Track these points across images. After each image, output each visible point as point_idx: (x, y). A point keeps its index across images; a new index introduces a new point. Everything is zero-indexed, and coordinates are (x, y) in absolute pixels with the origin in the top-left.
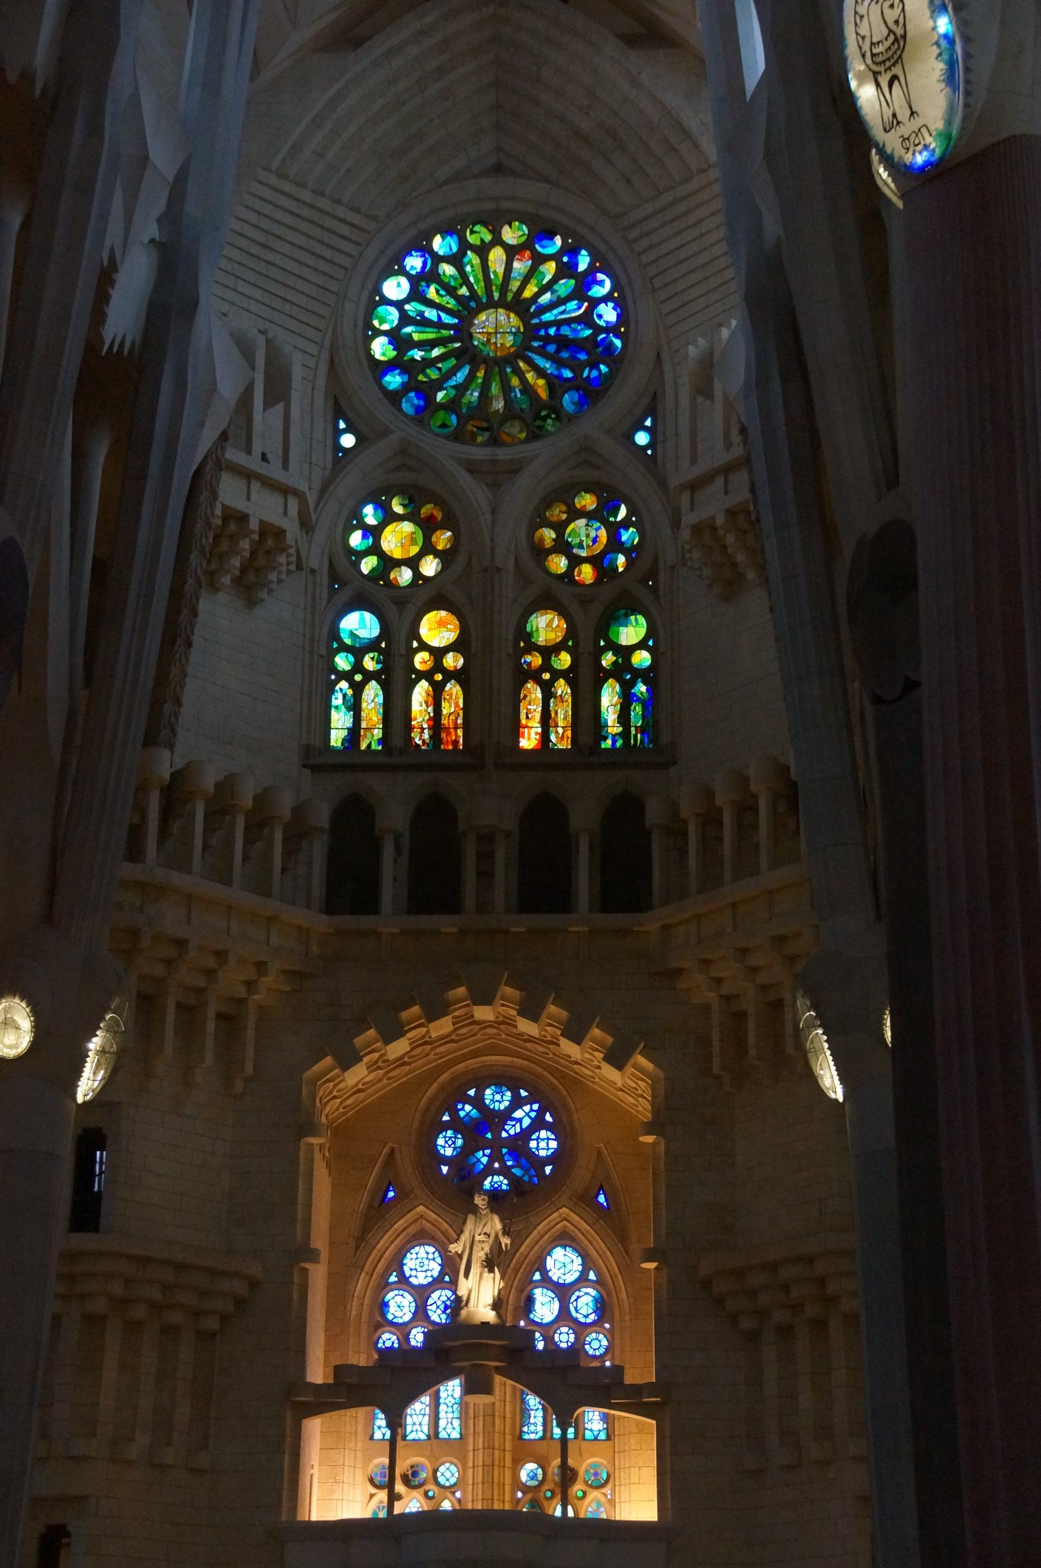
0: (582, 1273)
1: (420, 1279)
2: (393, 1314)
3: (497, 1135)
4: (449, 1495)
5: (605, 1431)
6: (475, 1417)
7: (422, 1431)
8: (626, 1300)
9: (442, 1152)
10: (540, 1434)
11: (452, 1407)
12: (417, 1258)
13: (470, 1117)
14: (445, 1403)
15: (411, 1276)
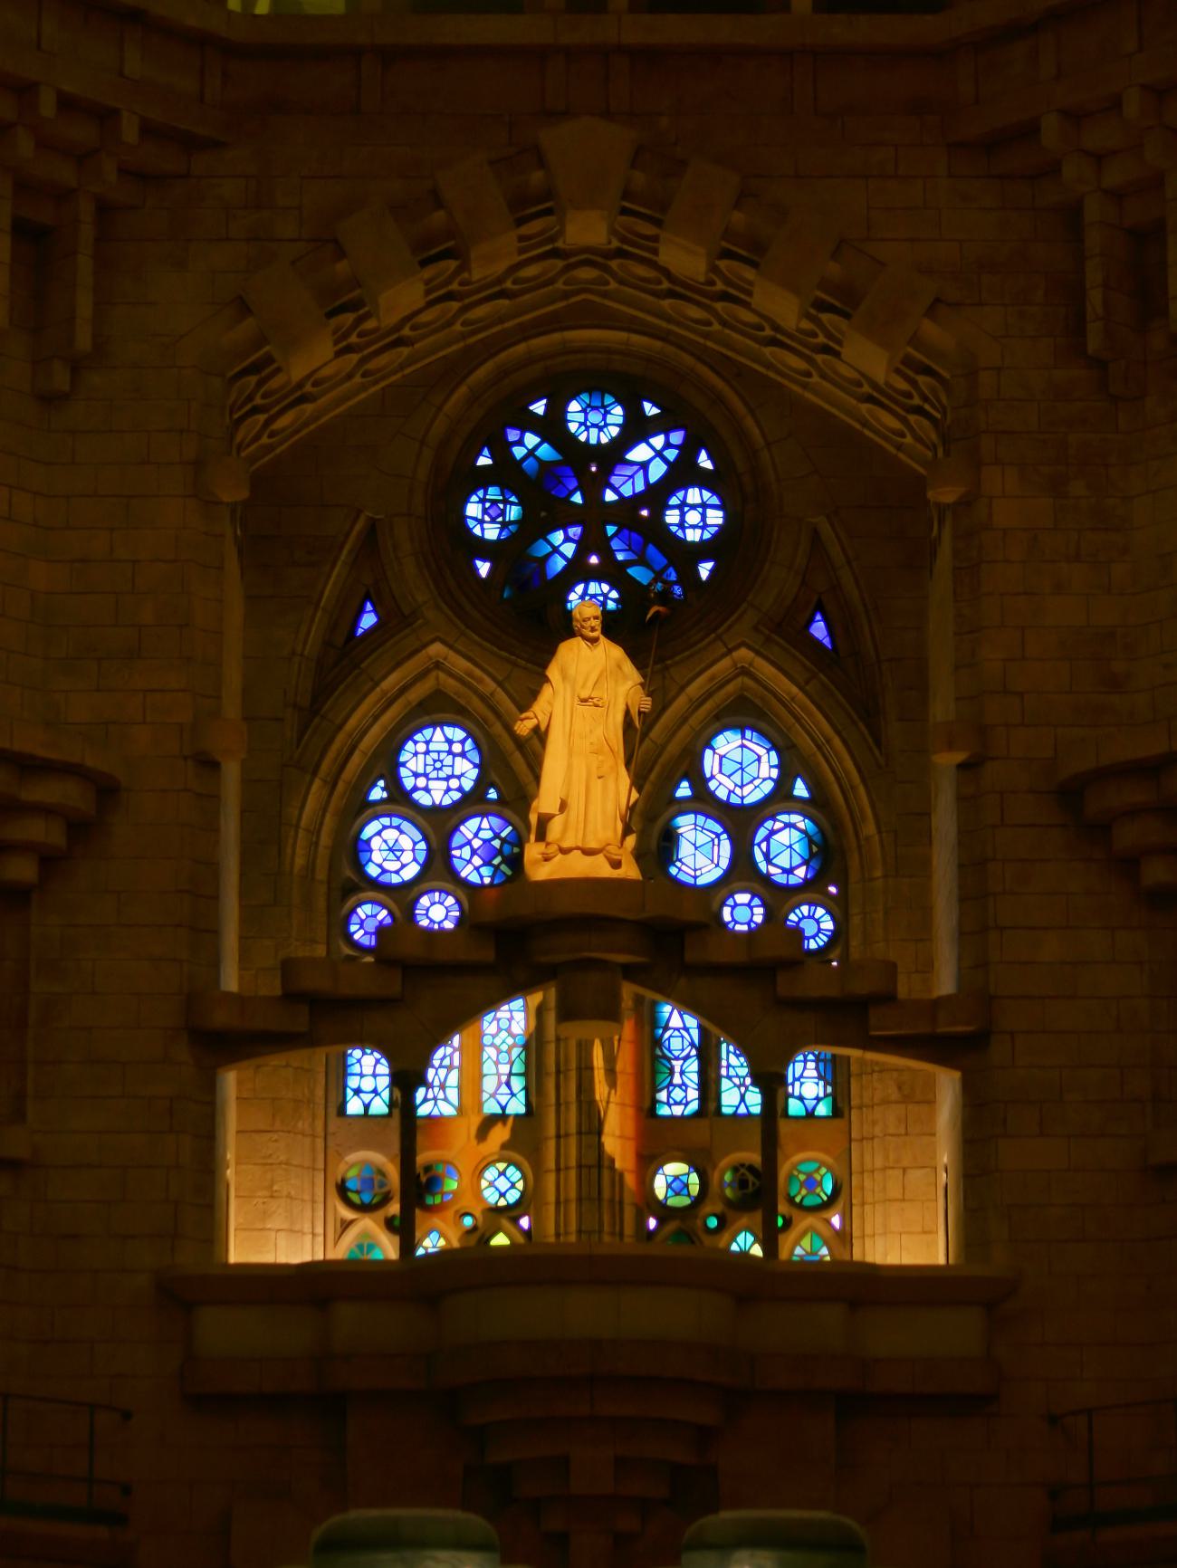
0: (778, 782)
1: (437, 794)
2: (380, 866)
3: (593, 496)
4: (505, 1223)
5: (830, 1100)
6: (558, 1072)
7: (446, 1099)
8: (877, 837)
9: (477, 531)
10: (694, 1106)
11: (509, 1052)
12: (427, 752)
13: (537, 458)
14: (492, 1045)
15: (415, 789)
